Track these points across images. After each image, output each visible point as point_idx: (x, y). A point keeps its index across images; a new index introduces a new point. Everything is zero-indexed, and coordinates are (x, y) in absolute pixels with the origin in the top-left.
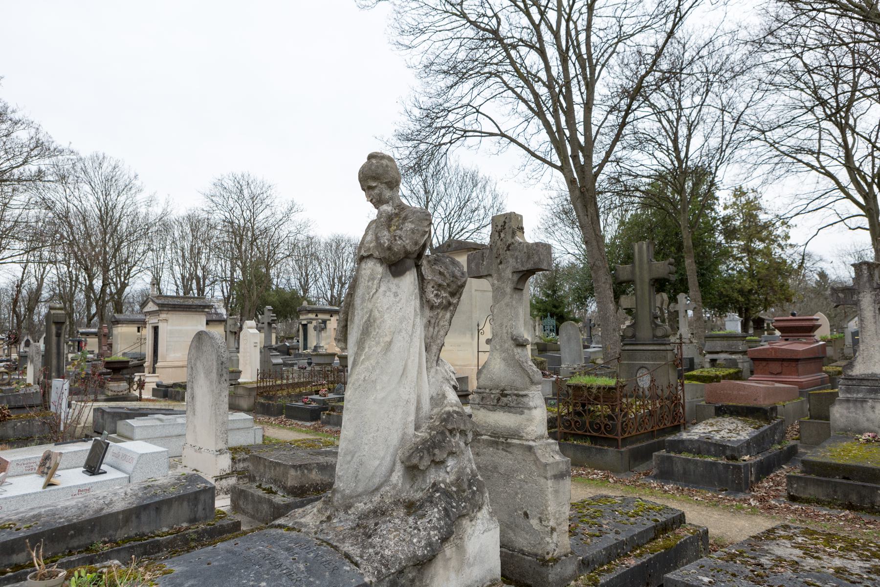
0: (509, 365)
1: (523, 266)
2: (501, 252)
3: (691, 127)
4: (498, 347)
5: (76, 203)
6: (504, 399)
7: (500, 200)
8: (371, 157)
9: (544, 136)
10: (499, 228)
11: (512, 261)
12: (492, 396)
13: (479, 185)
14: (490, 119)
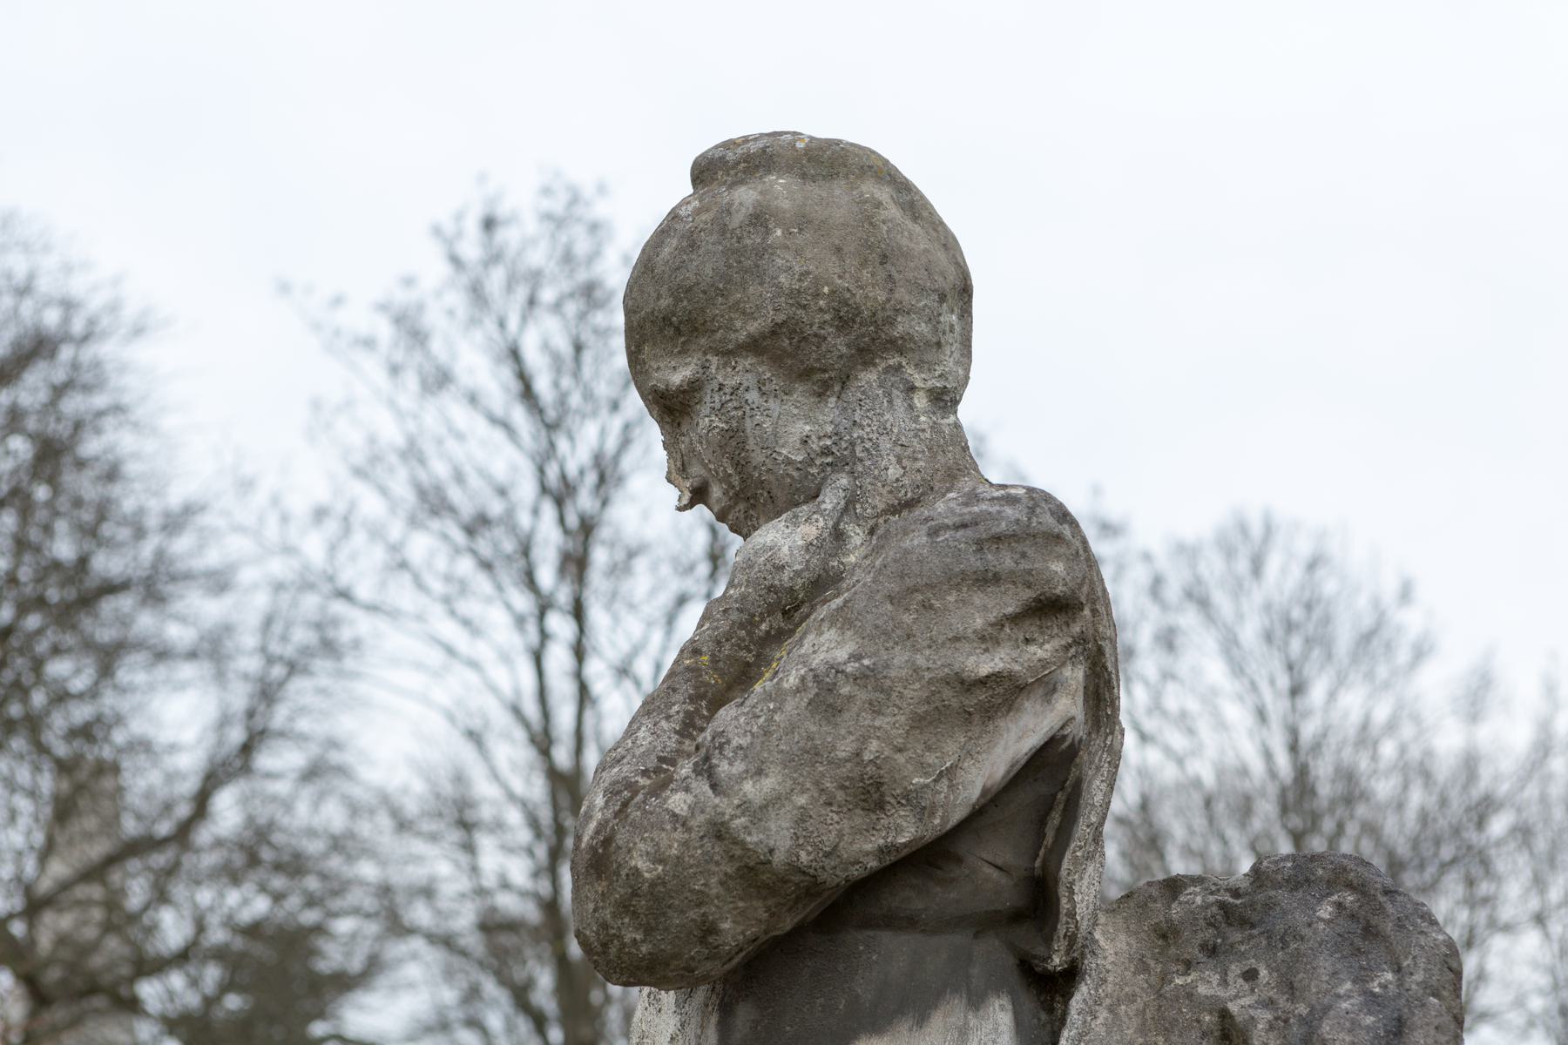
5: (1178, 741)
8: (705, 171)
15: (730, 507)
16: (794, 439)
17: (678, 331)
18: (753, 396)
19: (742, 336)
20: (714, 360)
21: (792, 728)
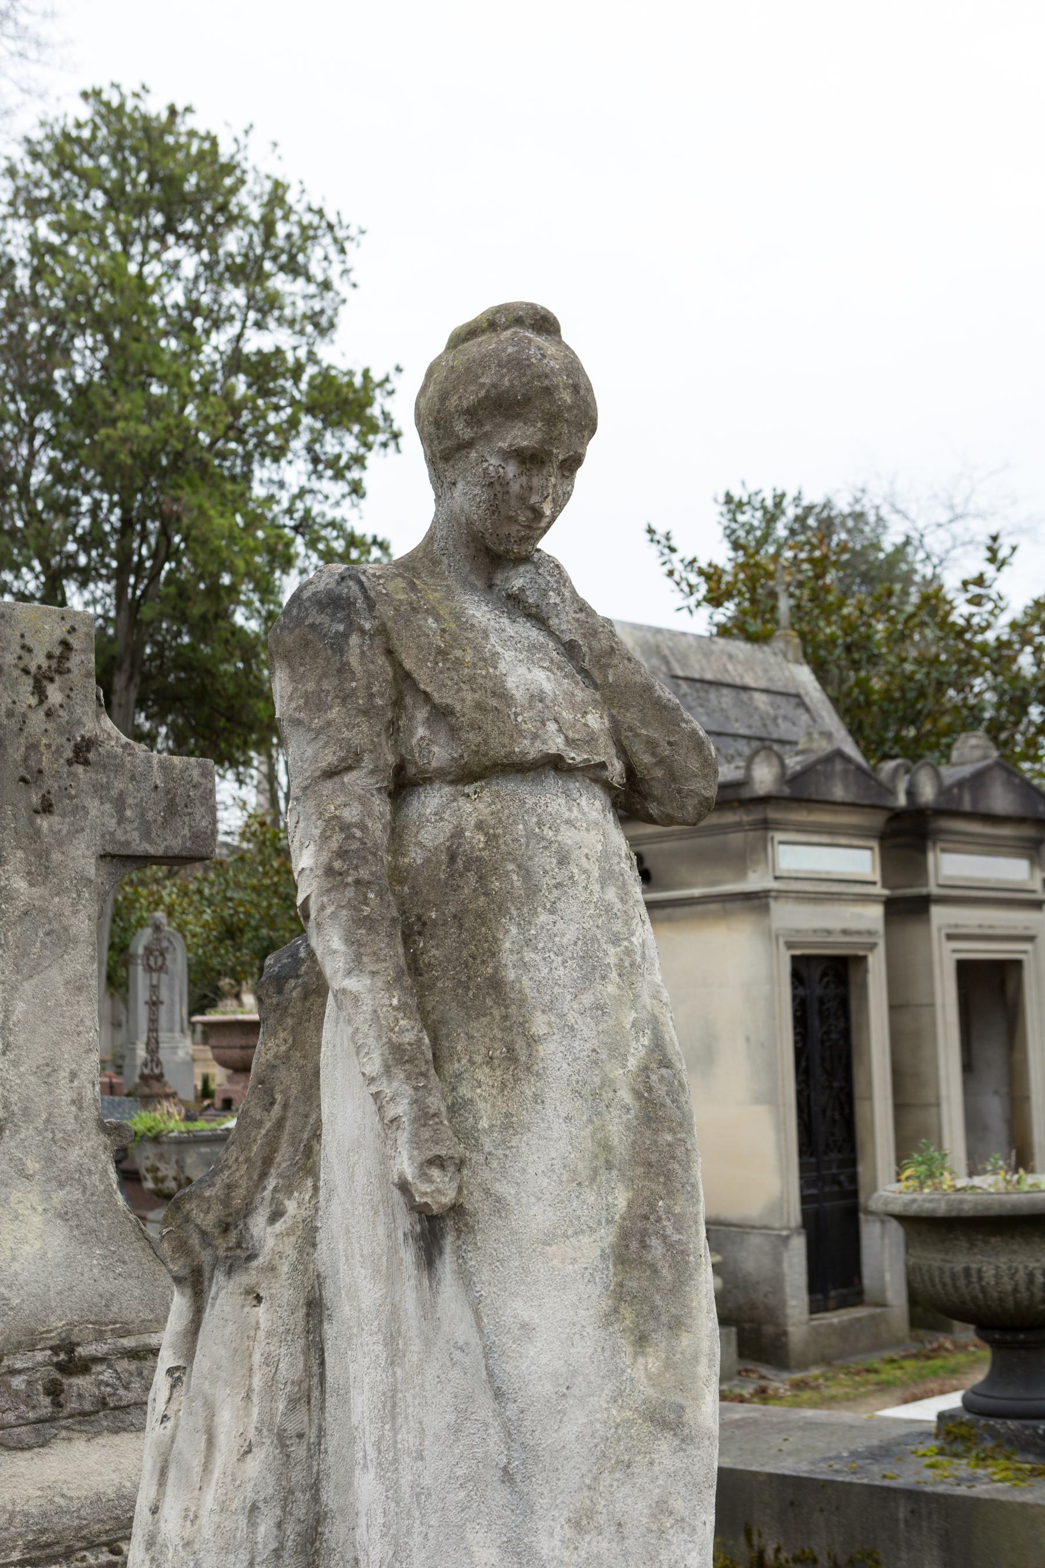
0: (87, 1236)
1: (146, 835)
2: (46, 760)
4: (32, 1166)
6: (80, 1383)
10: (38, 660)
11: (96, 810)
12: (18, 1382)
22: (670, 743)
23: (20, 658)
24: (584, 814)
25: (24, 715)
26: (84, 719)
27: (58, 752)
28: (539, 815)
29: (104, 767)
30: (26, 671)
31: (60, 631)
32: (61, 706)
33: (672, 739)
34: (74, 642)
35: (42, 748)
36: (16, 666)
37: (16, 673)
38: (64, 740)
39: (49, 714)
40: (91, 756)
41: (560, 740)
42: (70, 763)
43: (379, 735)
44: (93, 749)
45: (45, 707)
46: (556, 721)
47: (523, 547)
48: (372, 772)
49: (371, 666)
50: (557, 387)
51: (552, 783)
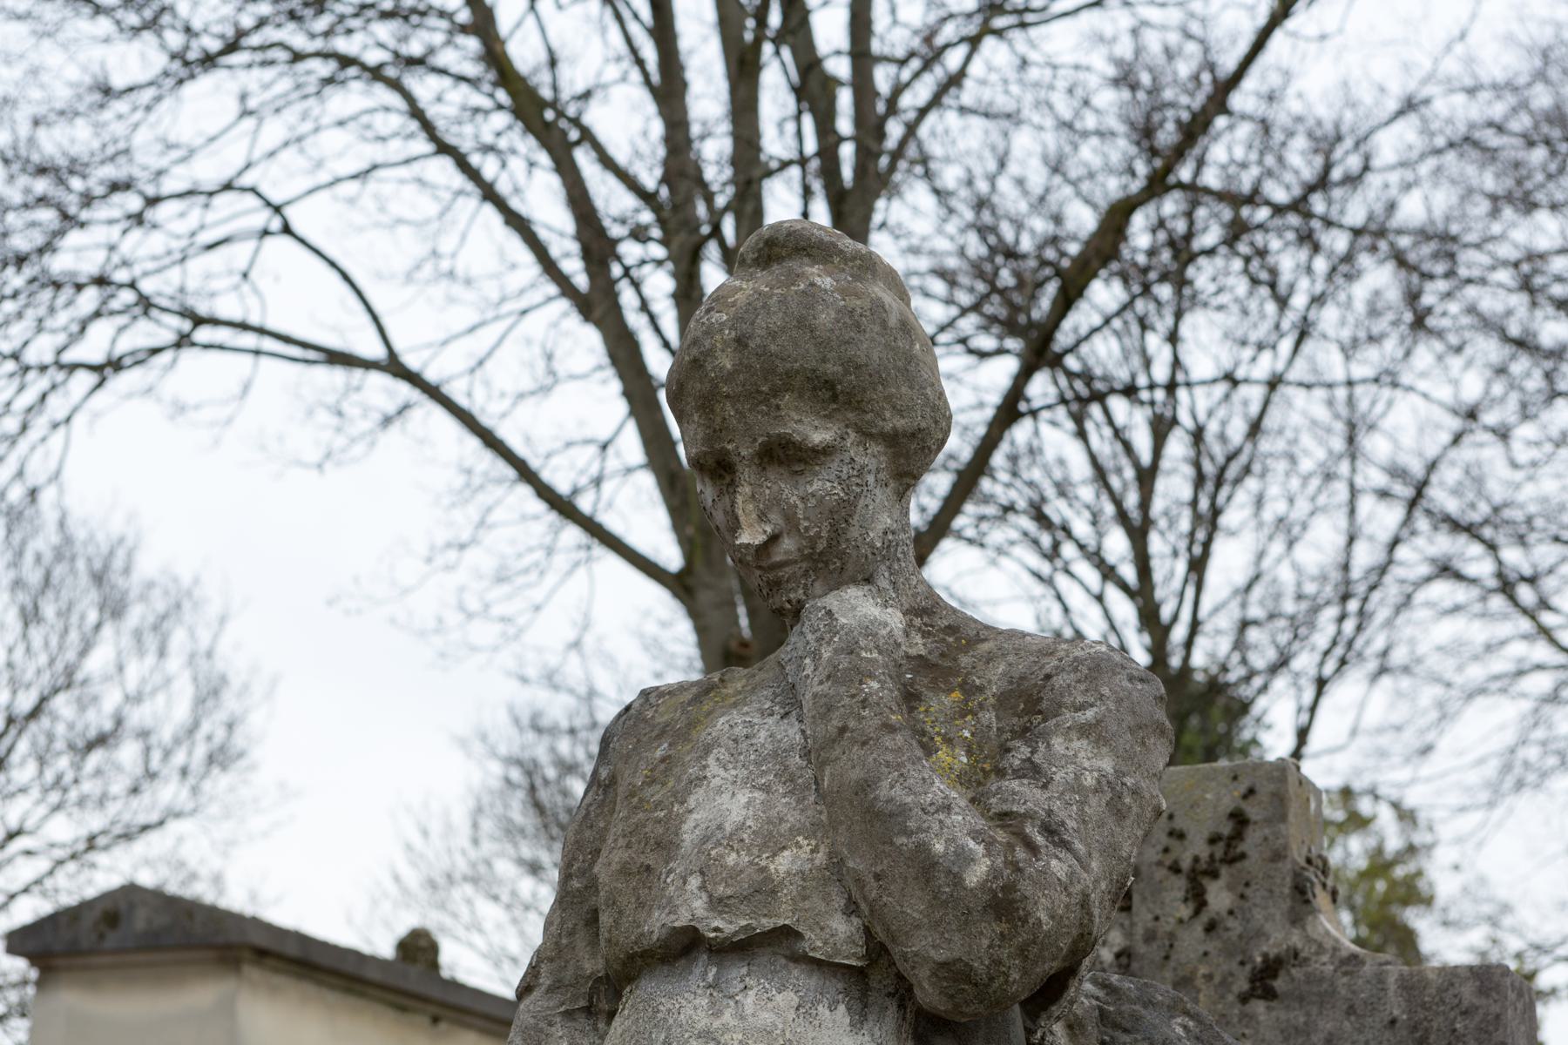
3: (1213, 481)
7: (230, 703)
9: (605, 404)
10: (1196, 848)
13: (136, 615)
14: (346, 277)
15: (796, 562)
16: (880, 527)
17: (834, 398)
18: (871, 479)
19: (888, 427)
20: (853, 435)
21: (1101, 824)
22: (877, 877)
23: (1166, 850)
24: (742, 1018)
25: (1172, 936)
26: (1268, 927)
27: (1225, 984)
28: (669, 1029)
29: (1301, 999)
30: (1175, 869)
31: (1229, 798)
32: (1231, 912)
33: (879, 869)
34: (1253, 811)
35: (1199, 982)
36: (1160, 863)
37: (1161, 873)
38: (1234, 966)
39: (1211, 927)
40: (1279, 984)
41: (699, 904)
42: (1244, 999)
43: (571, 934)
44: (1282, 973)
45: (1204, 918)
46: (702, 873)
47: (777, 599)
48: (551, 990)
49: (588, 833)
50: (710, 353)
51: (704, 971)
